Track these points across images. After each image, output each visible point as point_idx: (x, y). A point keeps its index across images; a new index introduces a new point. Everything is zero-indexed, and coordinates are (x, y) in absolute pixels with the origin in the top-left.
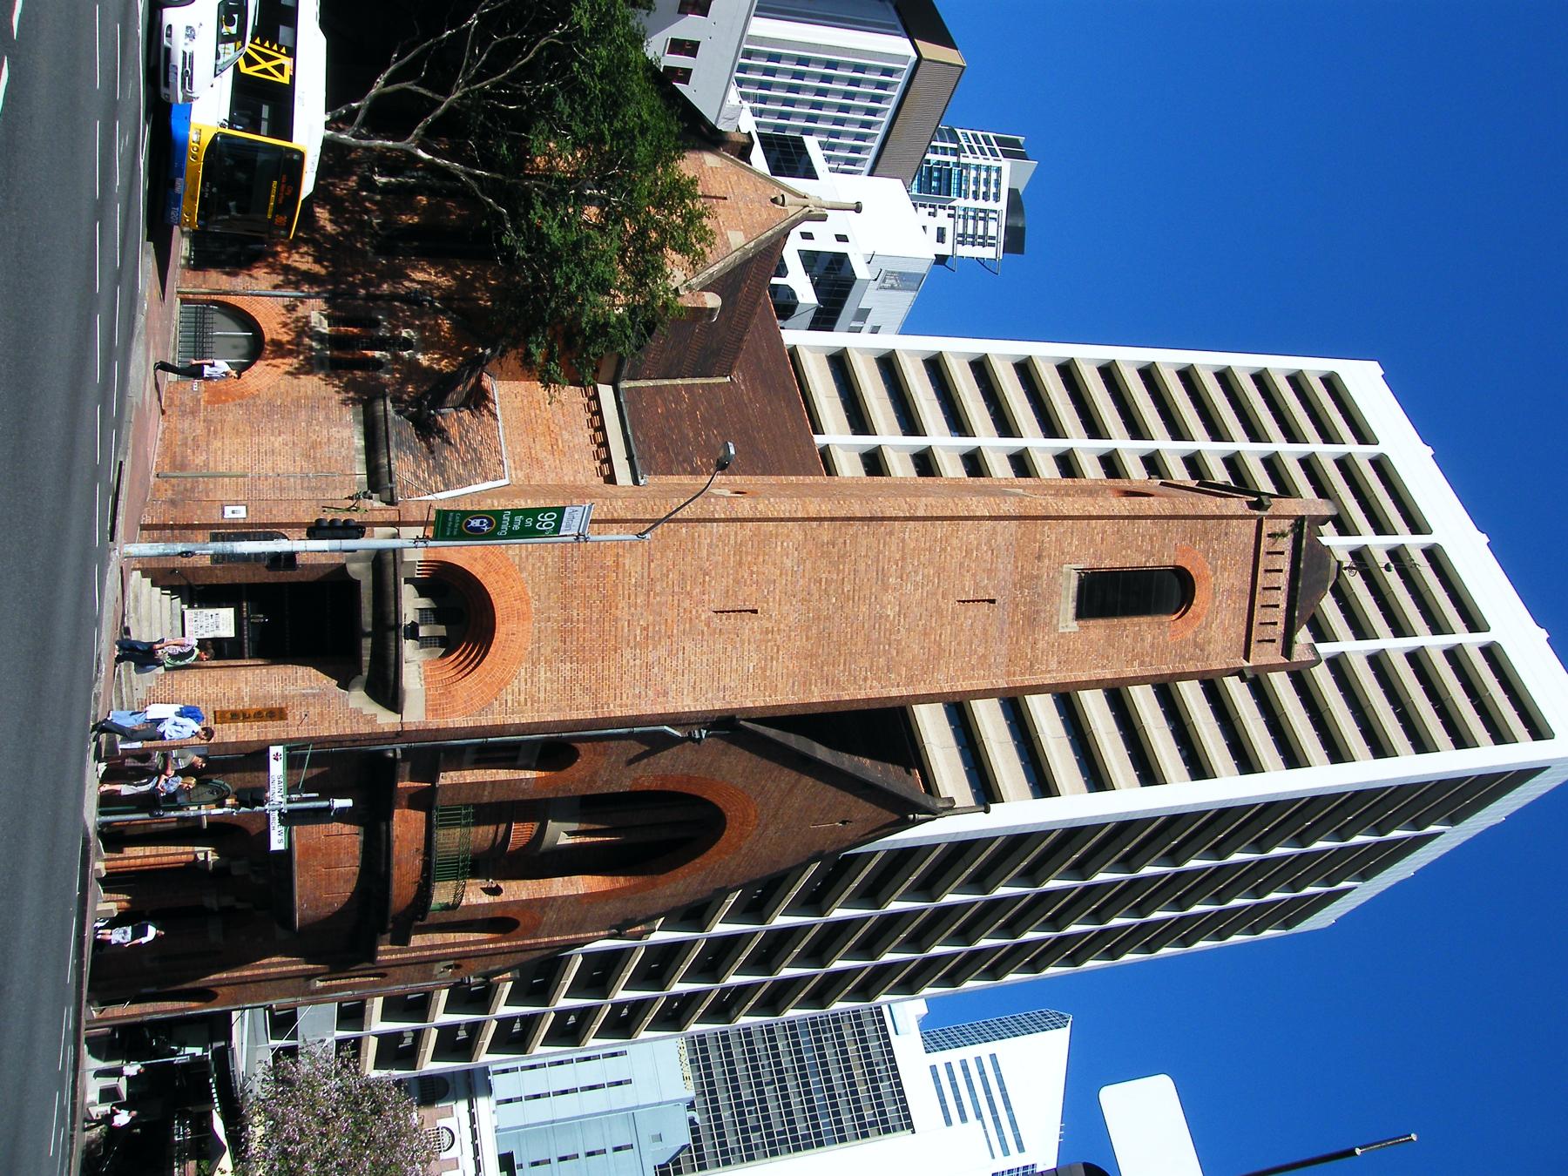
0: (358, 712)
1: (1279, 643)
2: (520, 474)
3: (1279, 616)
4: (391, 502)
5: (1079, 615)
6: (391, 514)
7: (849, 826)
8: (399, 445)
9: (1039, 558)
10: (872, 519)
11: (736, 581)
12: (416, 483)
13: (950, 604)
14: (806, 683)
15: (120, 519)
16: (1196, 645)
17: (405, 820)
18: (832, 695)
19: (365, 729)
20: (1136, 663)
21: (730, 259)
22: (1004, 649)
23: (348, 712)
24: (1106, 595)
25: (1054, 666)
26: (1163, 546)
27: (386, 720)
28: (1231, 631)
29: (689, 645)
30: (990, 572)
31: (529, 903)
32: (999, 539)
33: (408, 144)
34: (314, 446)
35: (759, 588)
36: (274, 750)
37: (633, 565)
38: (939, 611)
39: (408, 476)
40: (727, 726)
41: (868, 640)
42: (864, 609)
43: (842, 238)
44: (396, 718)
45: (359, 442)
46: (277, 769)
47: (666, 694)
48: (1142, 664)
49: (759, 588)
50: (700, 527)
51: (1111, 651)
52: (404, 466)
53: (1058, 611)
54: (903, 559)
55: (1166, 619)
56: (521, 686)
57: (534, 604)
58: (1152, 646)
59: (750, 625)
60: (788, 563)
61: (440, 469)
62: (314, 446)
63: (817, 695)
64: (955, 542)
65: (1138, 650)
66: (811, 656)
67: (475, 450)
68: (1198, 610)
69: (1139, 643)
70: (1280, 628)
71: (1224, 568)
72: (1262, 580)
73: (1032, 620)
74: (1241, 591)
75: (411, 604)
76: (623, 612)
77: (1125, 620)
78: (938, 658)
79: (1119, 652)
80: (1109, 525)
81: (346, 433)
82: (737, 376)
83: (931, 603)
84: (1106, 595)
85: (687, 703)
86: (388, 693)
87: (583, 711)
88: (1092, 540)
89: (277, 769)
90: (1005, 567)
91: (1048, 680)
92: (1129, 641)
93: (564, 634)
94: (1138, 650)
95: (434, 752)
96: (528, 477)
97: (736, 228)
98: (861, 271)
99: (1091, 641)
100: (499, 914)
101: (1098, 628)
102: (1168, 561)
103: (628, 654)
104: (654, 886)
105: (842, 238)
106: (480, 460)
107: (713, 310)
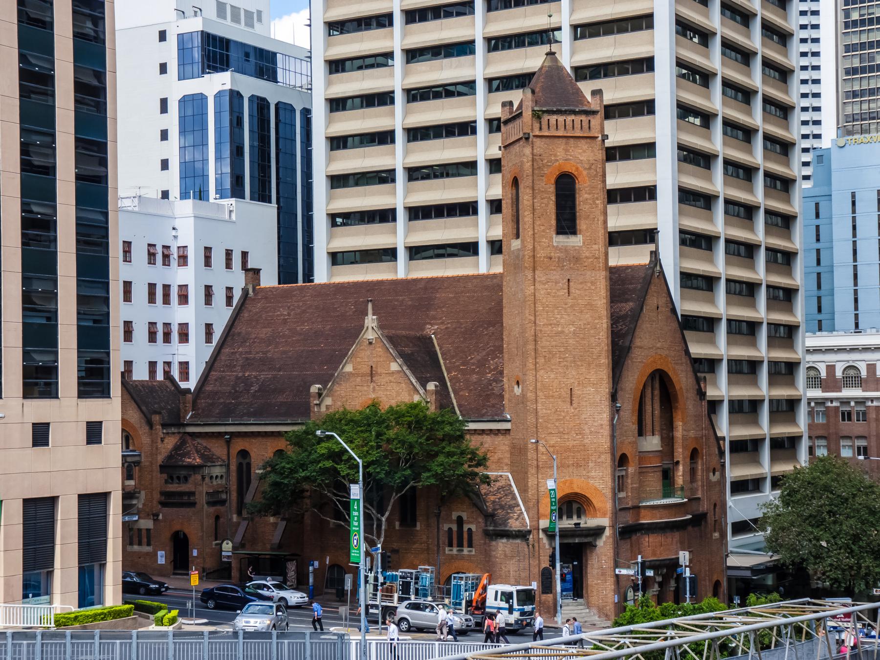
0: (605, 543)
1: (590, 118)
2: (505, 468)
3: (578, 119)
4: (529, 532)
5: (574, 233)
6: (535, 532)
7: (660, 304)
8: (506, 526)
9: (551, 258)
10: (535, 341)
11: (560, 398)
12: (520, 519)
13: (570, 301)
14: (599, 365)
15: (550, 625)
16: (590, 168)
17: (644, 518)
18: (604, 354)
19: (611, 540)
20: (598, 202)
21: (408, 372)
22: (589, 273)
23: (605, 545)
24: (567, 222)
25: (596, 247)
26: (546, 192)
27: (608, 532)
28: (585, 147)
29: (583, 416)
30: (556, 283)
31: (684, 448)
32: (543, 279)
33: (384, 519)
34: (506, 556)
35: (562, 388)
36: (617, 571)
37: (553, 440)
38: (572, 306)
39: (517, 523)
40: (614, 397)
41: (583, 339)
42: (571, 341)
43: (163, 36)
44: (607, 529)
45: (504, 540)
46: (624, 572)
47: (602, 425)
48: (597, 199)
49: (562, 388)
50: (540, 414)
51: (592, 216)
52: (514, 525)
53: (573, 247)
54: (551, 325)
55: (577, 186)
56: (597, 482)
57: (567, 478)
58: (589, 194)
59: (577, 391)
60: (552, 376)
61: (511, 507)
62: (506, 556)
63: (605, 360)
64: (544, 301)
65: (591, 202)
66: (589, 365)
67: (499, 489)
68: (574, 168)
69: (587, 199)
70: (583, 118)
71: (555, 155)
72: (560, 133)
73: (577, 259)
74: (566, 144)
75: (567, 523)
76: (570, 443)
77: (578, 209)
78: (591, 305)
79: (591, 212)
80: (538, 223)
81: (500, 544)
82: (430, 330)
83: (569, 310)
84: (567, 222)
85: (605, 416)
86: (598, 531)
87: (607, 459)
88: (543, 231)
89: (624, 572)
90: (555, 275)
91: (603, 250)
92: (587, 207)
93: (578, 466)
94: (591, 202)
95: (619, 510)
96: (507, 465)
97: (389, 367)
98: (195, 25)
99: (587, 229)
100: (688, 460)
101: (582, 224)
102: (552, 188)
103: (586, 441)
104: (681, 388)
105: (163, 36)
106: (502, 487)
107: (436, 386)
